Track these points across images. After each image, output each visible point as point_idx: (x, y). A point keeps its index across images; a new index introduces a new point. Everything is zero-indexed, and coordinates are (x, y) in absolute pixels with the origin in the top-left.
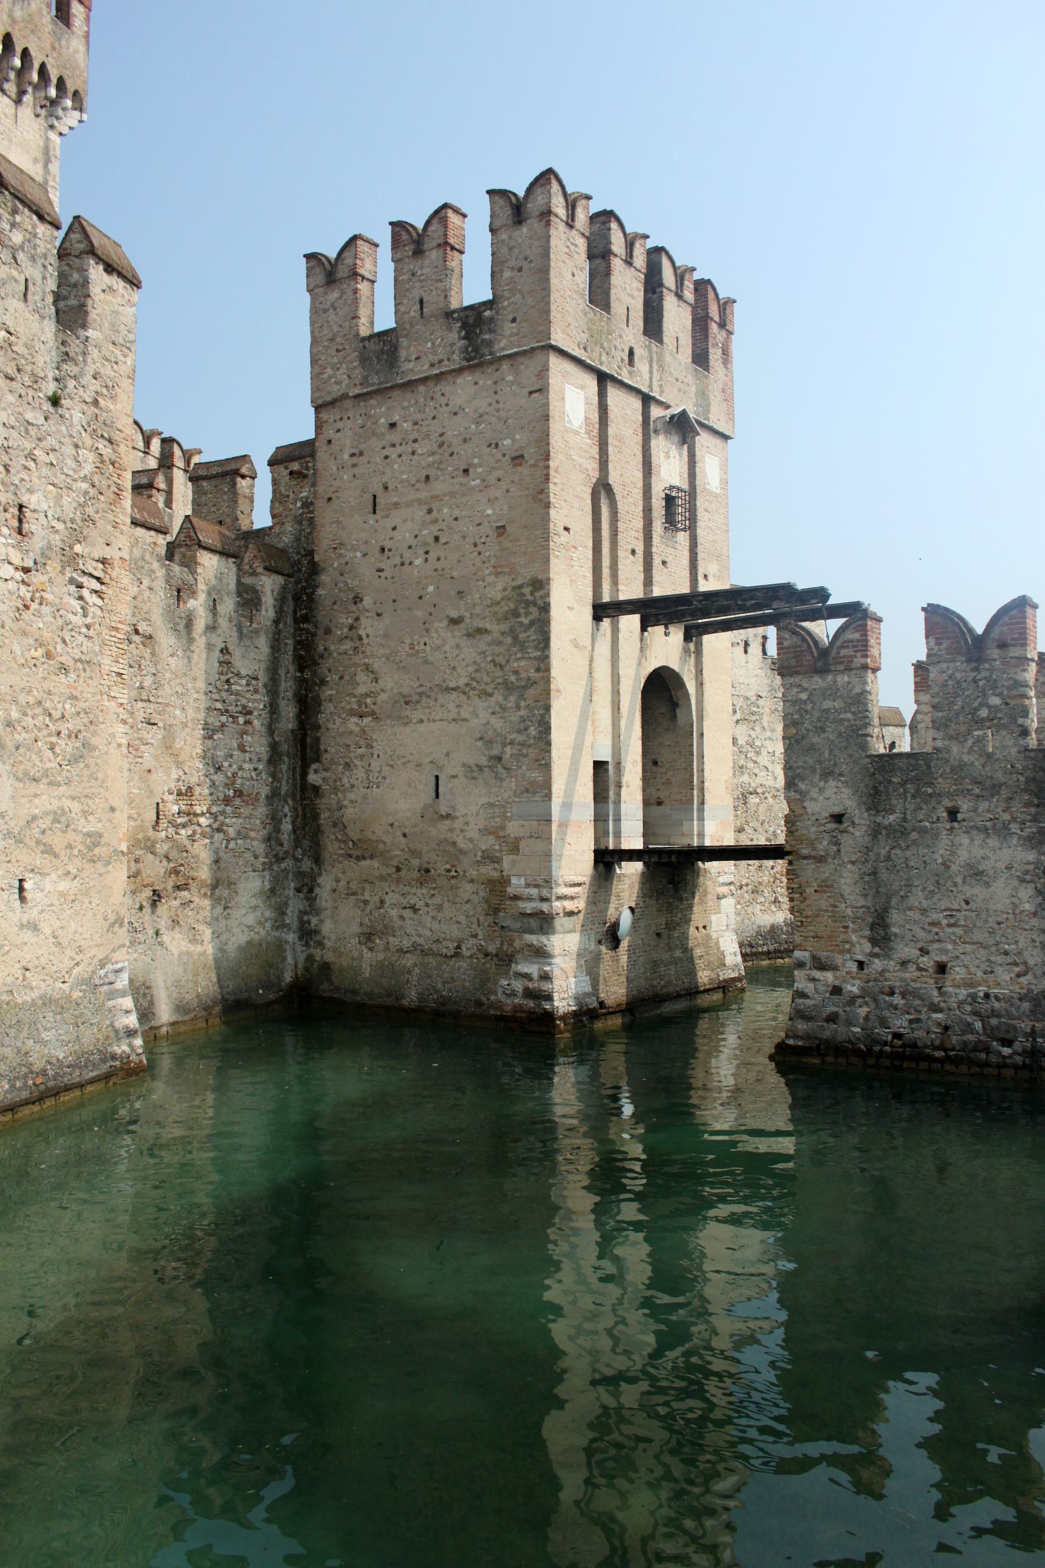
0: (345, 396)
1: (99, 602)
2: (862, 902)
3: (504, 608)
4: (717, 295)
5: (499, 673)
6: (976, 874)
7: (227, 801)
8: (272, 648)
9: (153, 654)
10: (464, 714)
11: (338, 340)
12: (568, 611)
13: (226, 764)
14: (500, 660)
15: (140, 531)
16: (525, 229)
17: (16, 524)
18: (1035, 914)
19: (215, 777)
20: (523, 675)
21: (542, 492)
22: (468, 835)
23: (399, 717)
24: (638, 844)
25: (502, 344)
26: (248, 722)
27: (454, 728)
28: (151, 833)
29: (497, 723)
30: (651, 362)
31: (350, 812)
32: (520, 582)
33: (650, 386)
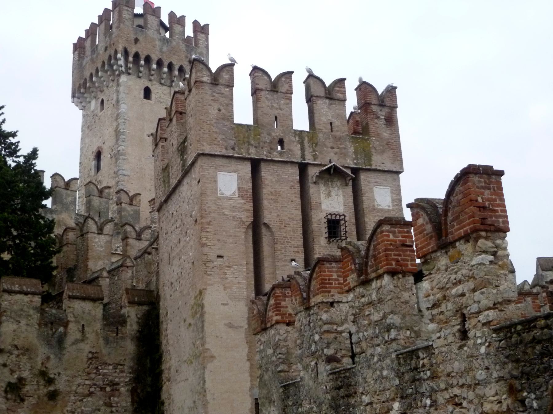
9: (30, 358)
12: (222, 306)
30: (302, 144)
33: (303, 157)
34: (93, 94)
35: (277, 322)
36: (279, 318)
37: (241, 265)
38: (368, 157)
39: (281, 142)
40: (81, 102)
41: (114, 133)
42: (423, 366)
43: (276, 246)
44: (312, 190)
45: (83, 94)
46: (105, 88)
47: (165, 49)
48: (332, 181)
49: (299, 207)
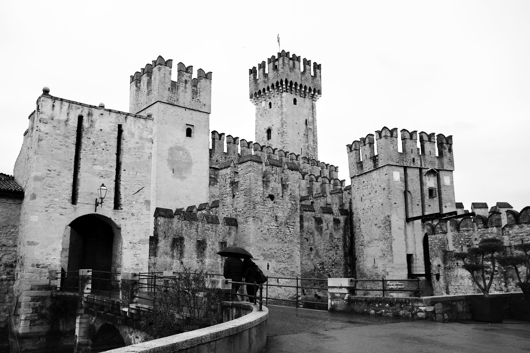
0: (355, 176)
1: (293, 230)
2: (444, 284)
3: (384, 221)
4: (445, 137)
5: (383, 236)
6: (462, 278)
7: (333, 265)
8: (344, 232)
9: (313, 236)
10: (379, 245)
11: (353, 164)
13: (332, 257)
14: (384, 233)
15: (308, 212)
16: (382, 139)
17: (275, 219)
18: (472, 286)
19: (329, 260)
20: (387, 236)
21: (388, 196)
22: (380, 271)
23: (368, 246)
24: (424, 273)
25: (380, 164)
26: (339, 248)
27: (377, 248)
28: (313, 272)
29: (384, 247)
31: (361, 267)
32: (386, 216)
33: (421, 165)
34: (264, 99)
35: (441, 233)
36: (441, 231)
37: (402, 206)
38: (443, 166)
39: (414, 159)
41: (280, 121)
42: (508, 251)
43: (413, 199)
44: (424, 178)
46: (272, 97)
47: (303, 78)
48: (430, 174)
49: (420, 185)
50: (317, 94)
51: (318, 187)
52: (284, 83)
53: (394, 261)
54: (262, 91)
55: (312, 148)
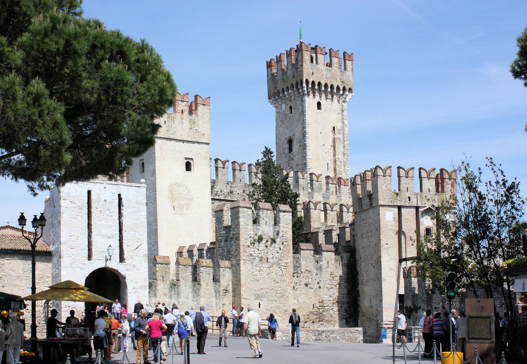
30: (417, 198)
34: (284, 101)
39: (409, 198)
40: (275, 104)
45: (277, 100)
50: (347, 93)
51: (333, 216)
52: (304, 85)
53: (383, 301)
54: (281, 92)
55: (341, 162)
